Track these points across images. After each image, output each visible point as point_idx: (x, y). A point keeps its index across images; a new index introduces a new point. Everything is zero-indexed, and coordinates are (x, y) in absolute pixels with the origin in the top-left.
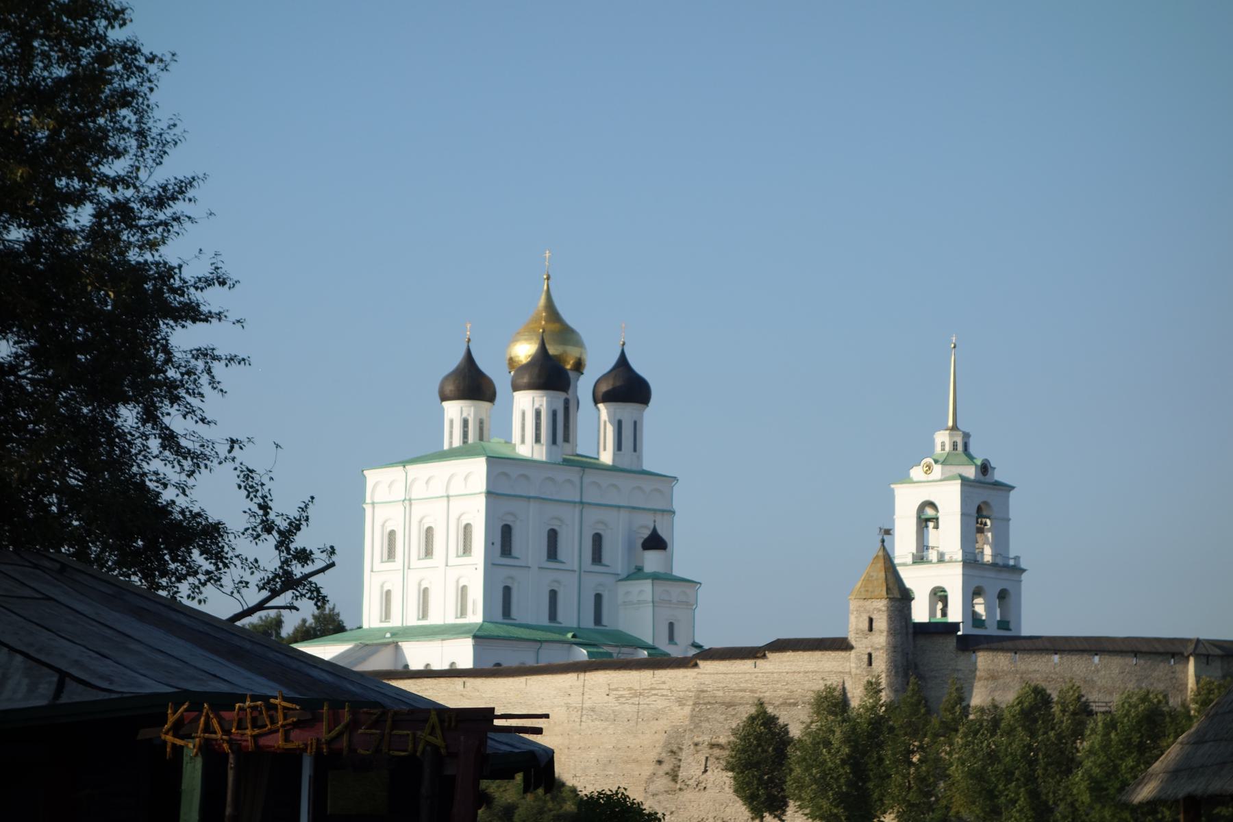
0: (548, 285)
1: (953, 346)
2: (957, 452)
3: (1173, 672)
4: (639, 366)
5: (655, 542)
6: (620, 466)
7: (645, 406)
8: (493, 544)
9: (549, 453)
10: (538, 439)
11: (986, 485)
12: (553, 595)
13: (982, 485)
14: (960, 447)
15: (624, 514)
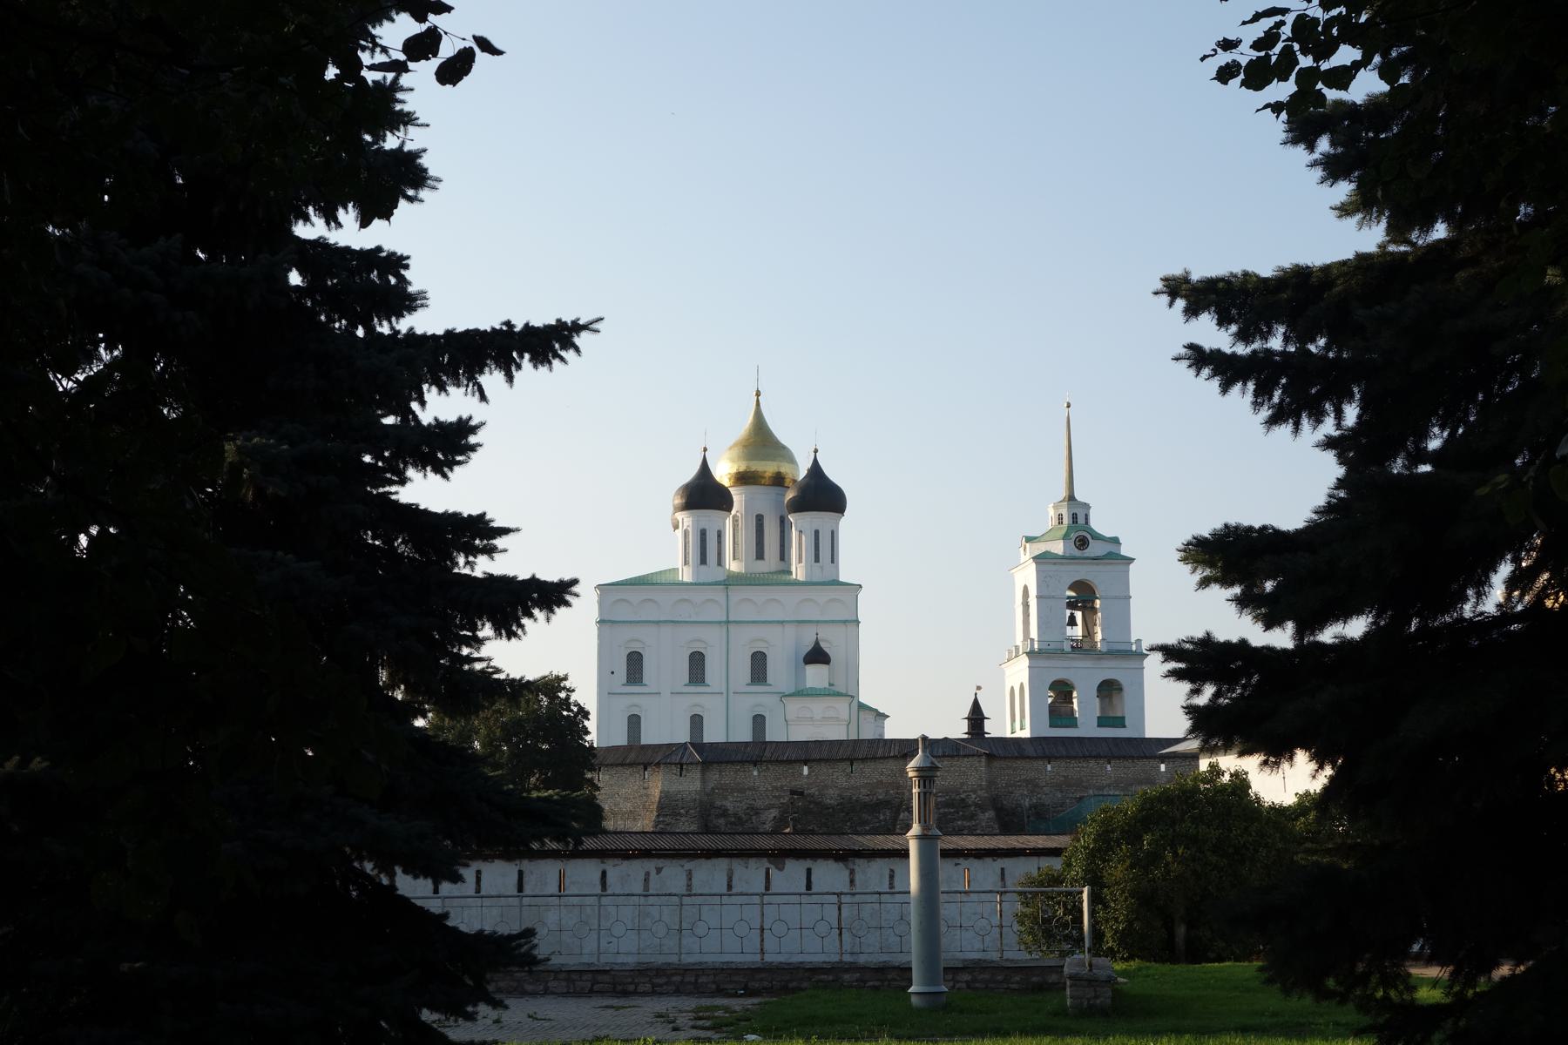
0: (758, 401)
1: (1066, 405)
2: (1062, 526)
3: (644, 788)
4: (833, 473)
5: (817, 656)
6: (815, 579)
7: (840, 515)
8: (613, 673)
9: (696, 573)
10: (686, 563)
11: (1081, 561)
12: (697, 722)
13: (1072, 561)
14: (1066, 521)
15: (790, 631)
